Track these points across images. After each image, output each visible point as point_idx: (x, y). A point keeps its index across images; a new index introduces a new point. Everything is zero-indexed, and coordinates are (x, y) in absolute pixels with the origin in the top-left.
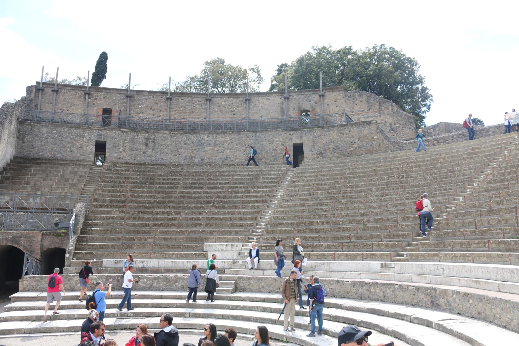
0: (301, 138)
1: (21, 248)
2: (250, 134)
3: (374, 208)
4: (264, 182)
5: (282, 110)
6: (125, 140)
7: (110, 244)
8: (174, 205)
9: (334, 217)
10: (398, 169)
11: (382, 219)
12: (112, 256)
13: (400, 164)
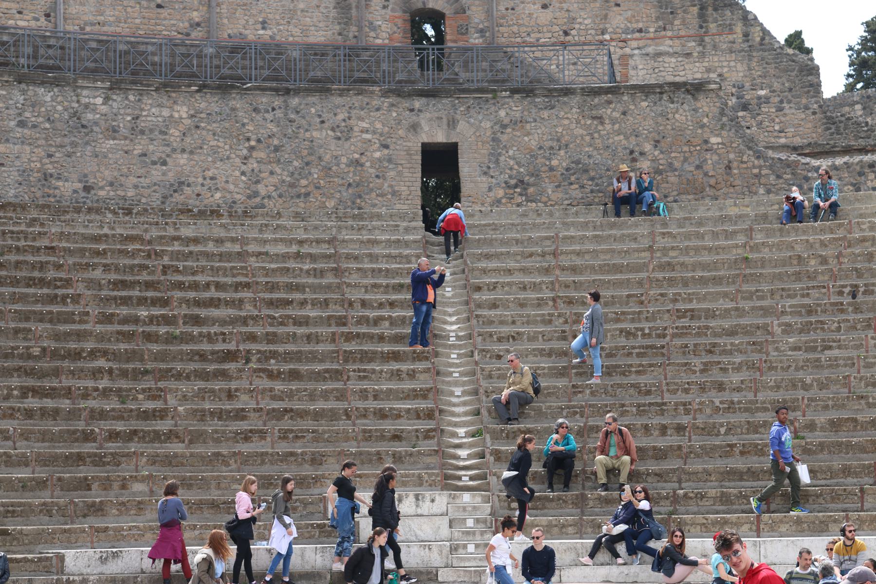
0: (452, 124)
2: (264, 100)
3: (806, 387)
4: (375, 286)
7: (37, 501)
8: (110, 364)
9: (687, 412)
10: (824, 261)
11: (855, 420)
12: (99, 536)
13: (823, 244)
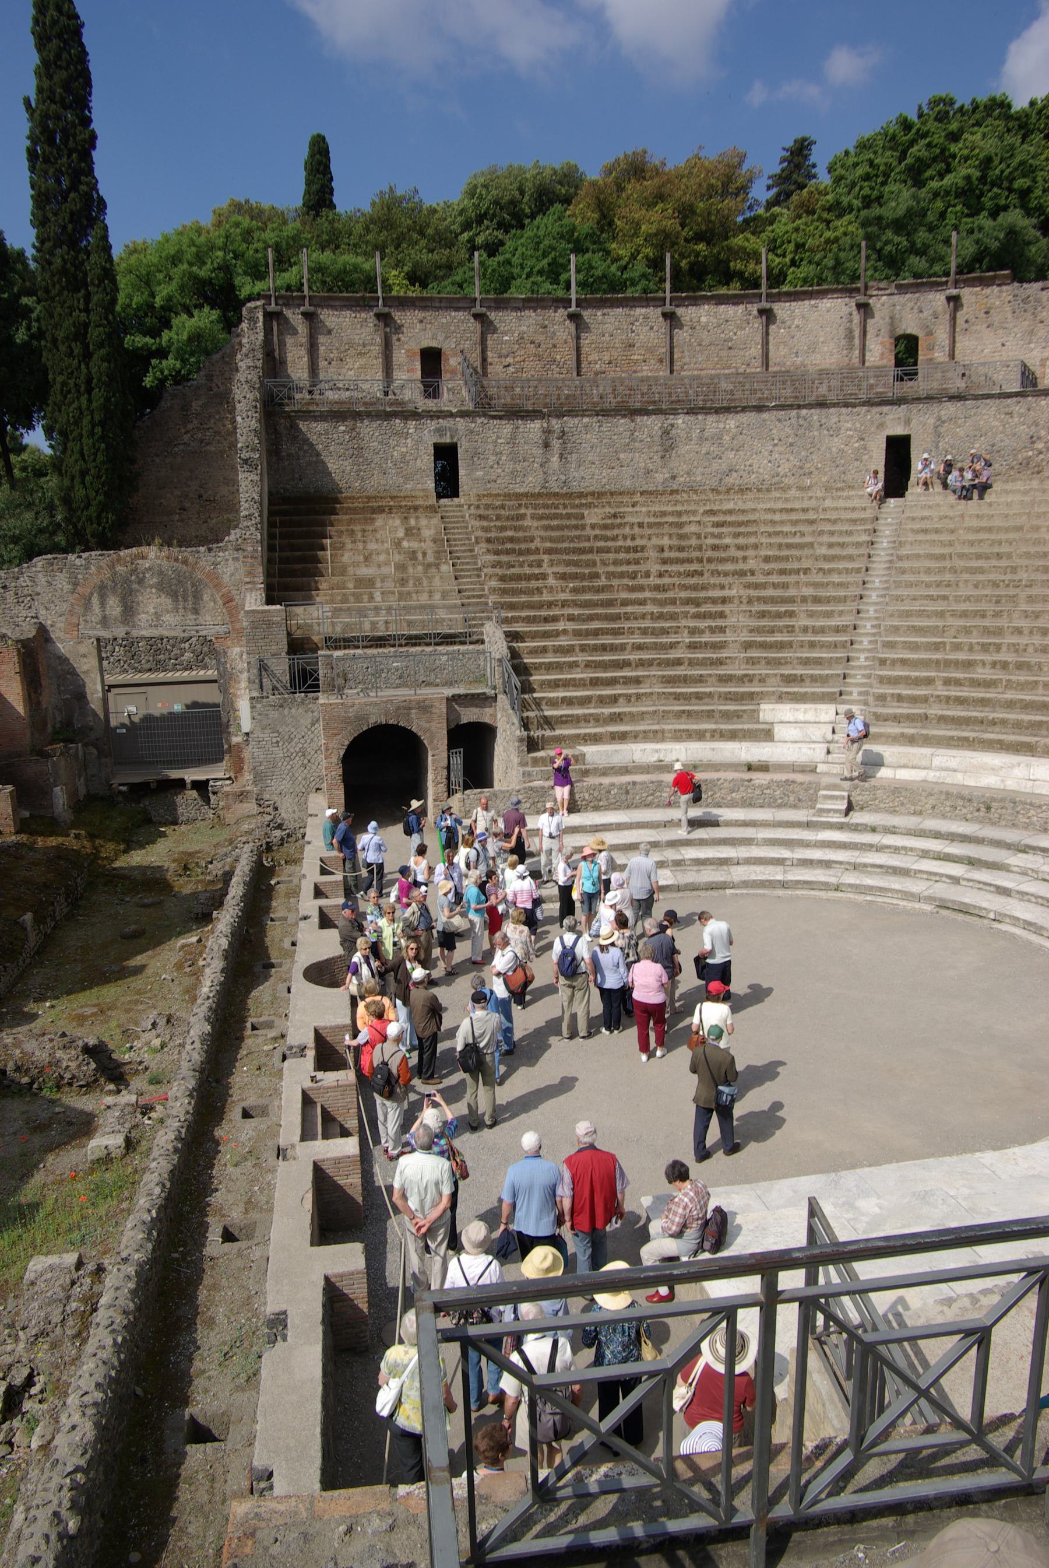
0: (908, 422)
1: (414, 729)
6: (498, 437)
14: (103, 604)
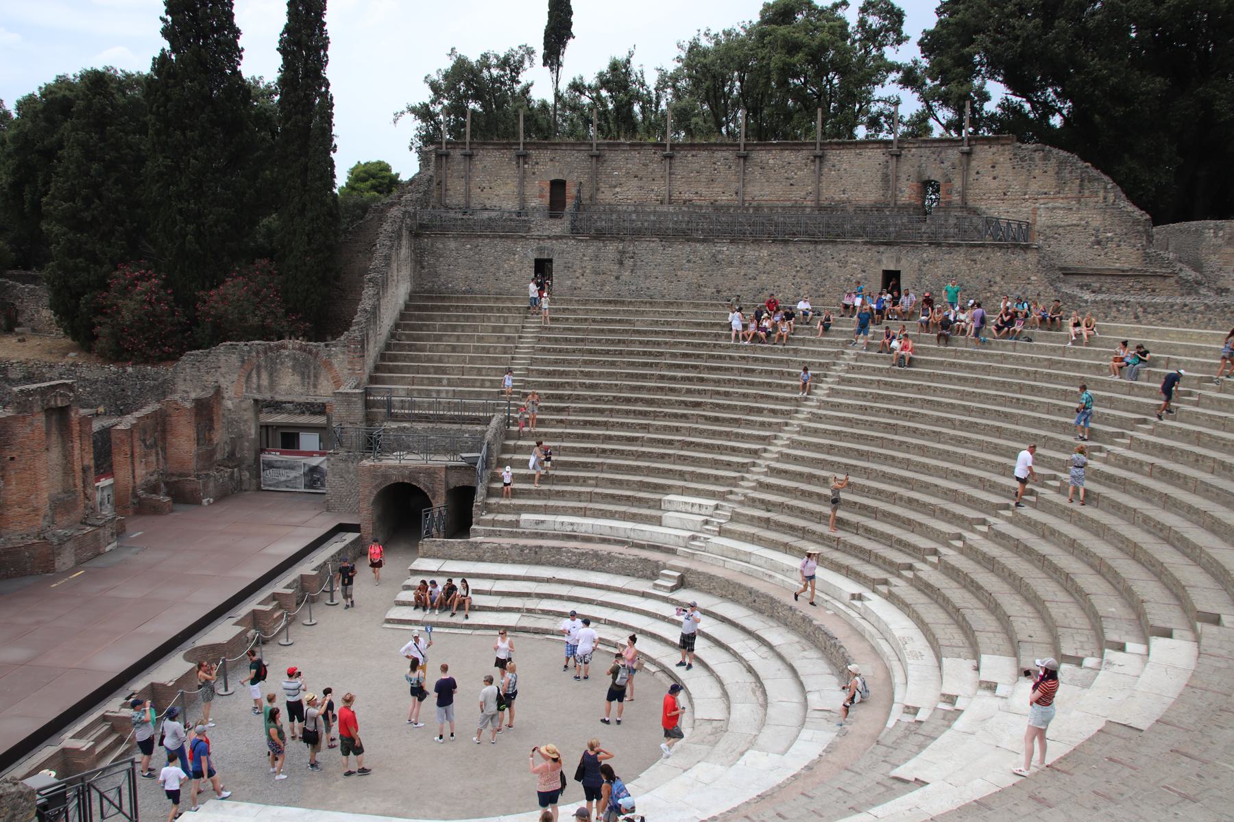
0: (898, 260)
5: (885, 178)
14: (259, 377)
